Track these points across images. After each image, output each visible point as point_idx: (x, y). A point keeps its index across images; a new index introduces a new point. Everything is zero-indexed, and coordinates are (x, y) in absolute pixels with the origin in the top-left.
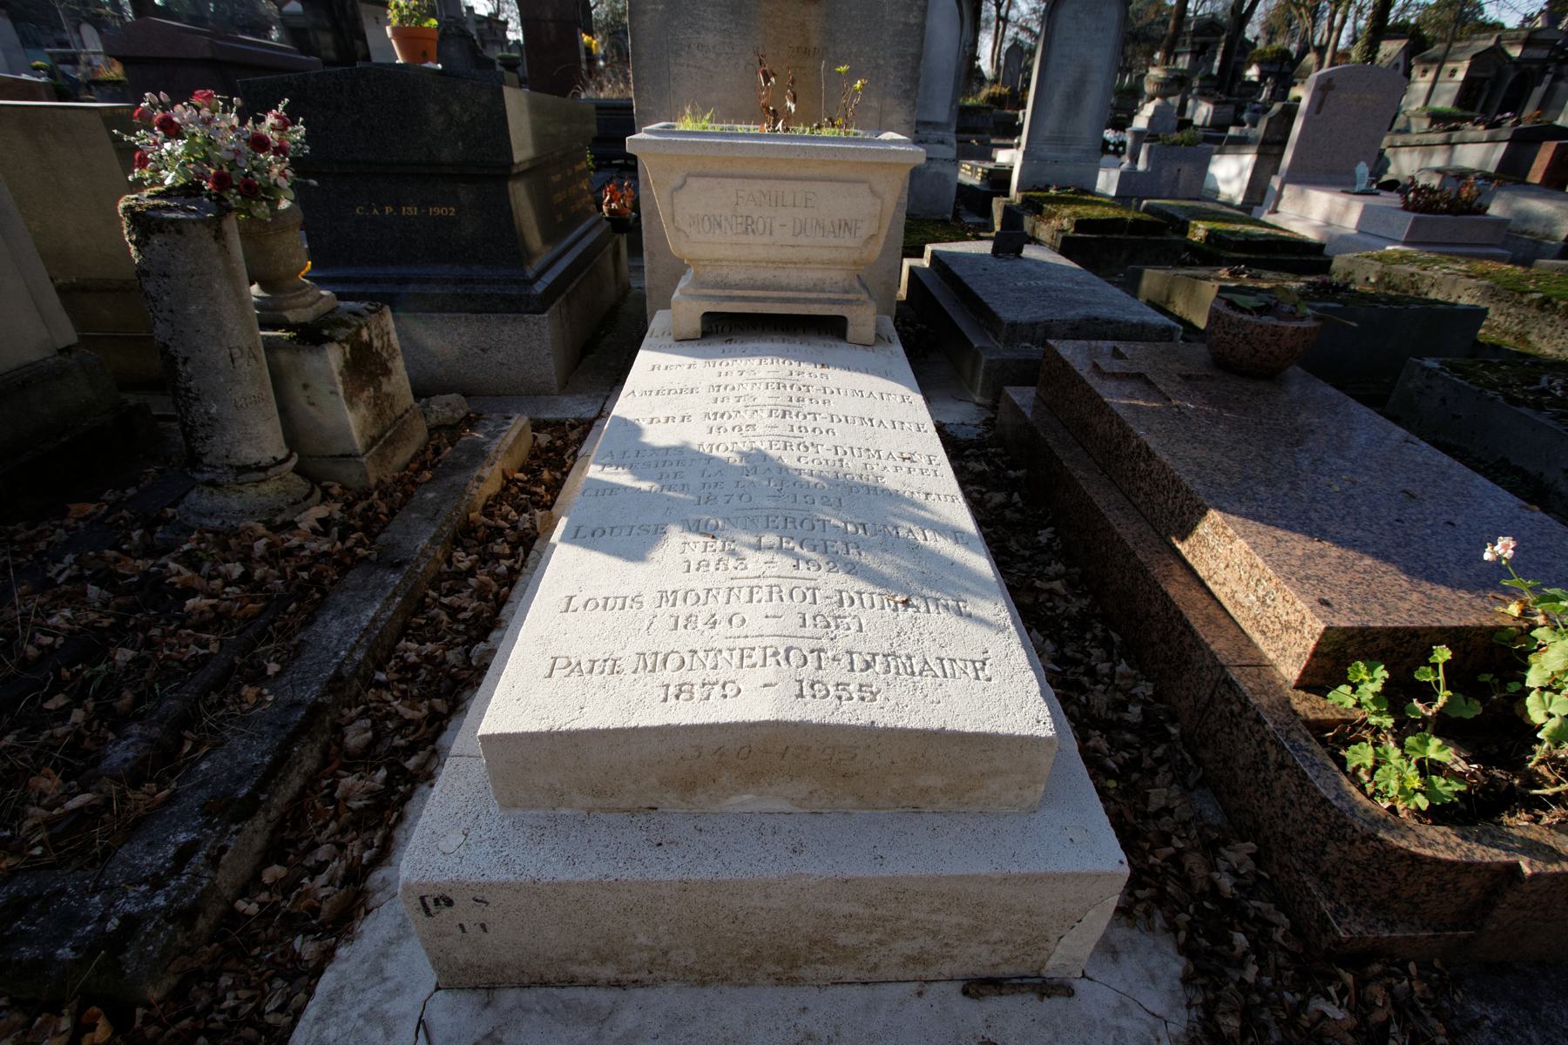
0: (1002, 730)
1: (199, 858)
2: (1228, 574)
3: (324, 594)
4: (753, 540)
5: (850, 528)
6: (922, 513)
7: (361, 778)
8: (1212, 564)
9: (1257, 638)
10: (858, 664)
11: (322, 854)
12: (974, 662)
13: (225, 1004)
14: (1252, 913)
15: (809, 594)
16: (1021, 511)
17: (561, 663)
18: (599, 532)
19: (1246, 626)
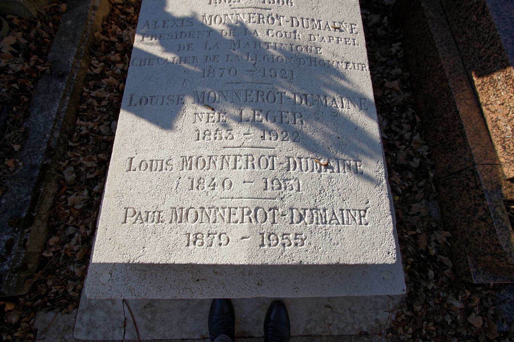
0: (369, 261)
1: (16, 247)
2: (500, 109)
3: (30, 96)
4: (237, 113)
5: (297, 99)
6: (343, 83)
7: (77, 195)
8: (492, 98)
9: (499, 148)
10: (296, 219)
11: (71, 230)
12: (360, 211)
13: (52, 291)
14: (438, 260)
15: (270, 161)
16: (386, 29)
17: (130, 212)
18: (144, 100)
19: (495, 140)
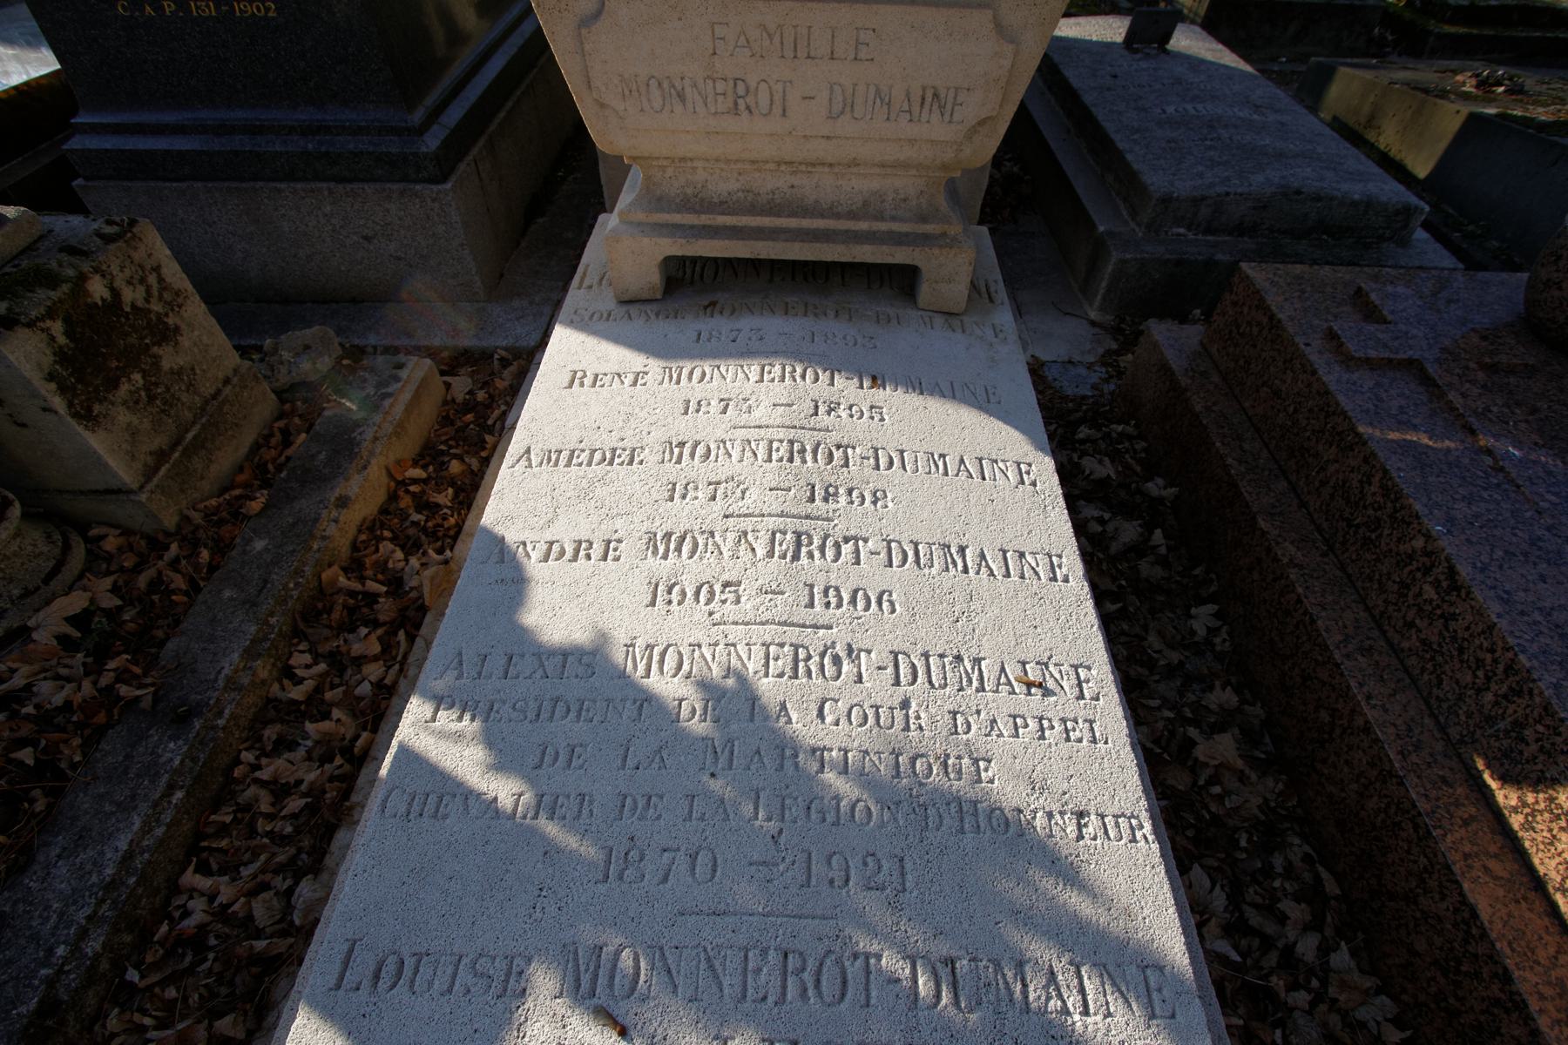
5: (924, 984)
16: (1164, 562)
